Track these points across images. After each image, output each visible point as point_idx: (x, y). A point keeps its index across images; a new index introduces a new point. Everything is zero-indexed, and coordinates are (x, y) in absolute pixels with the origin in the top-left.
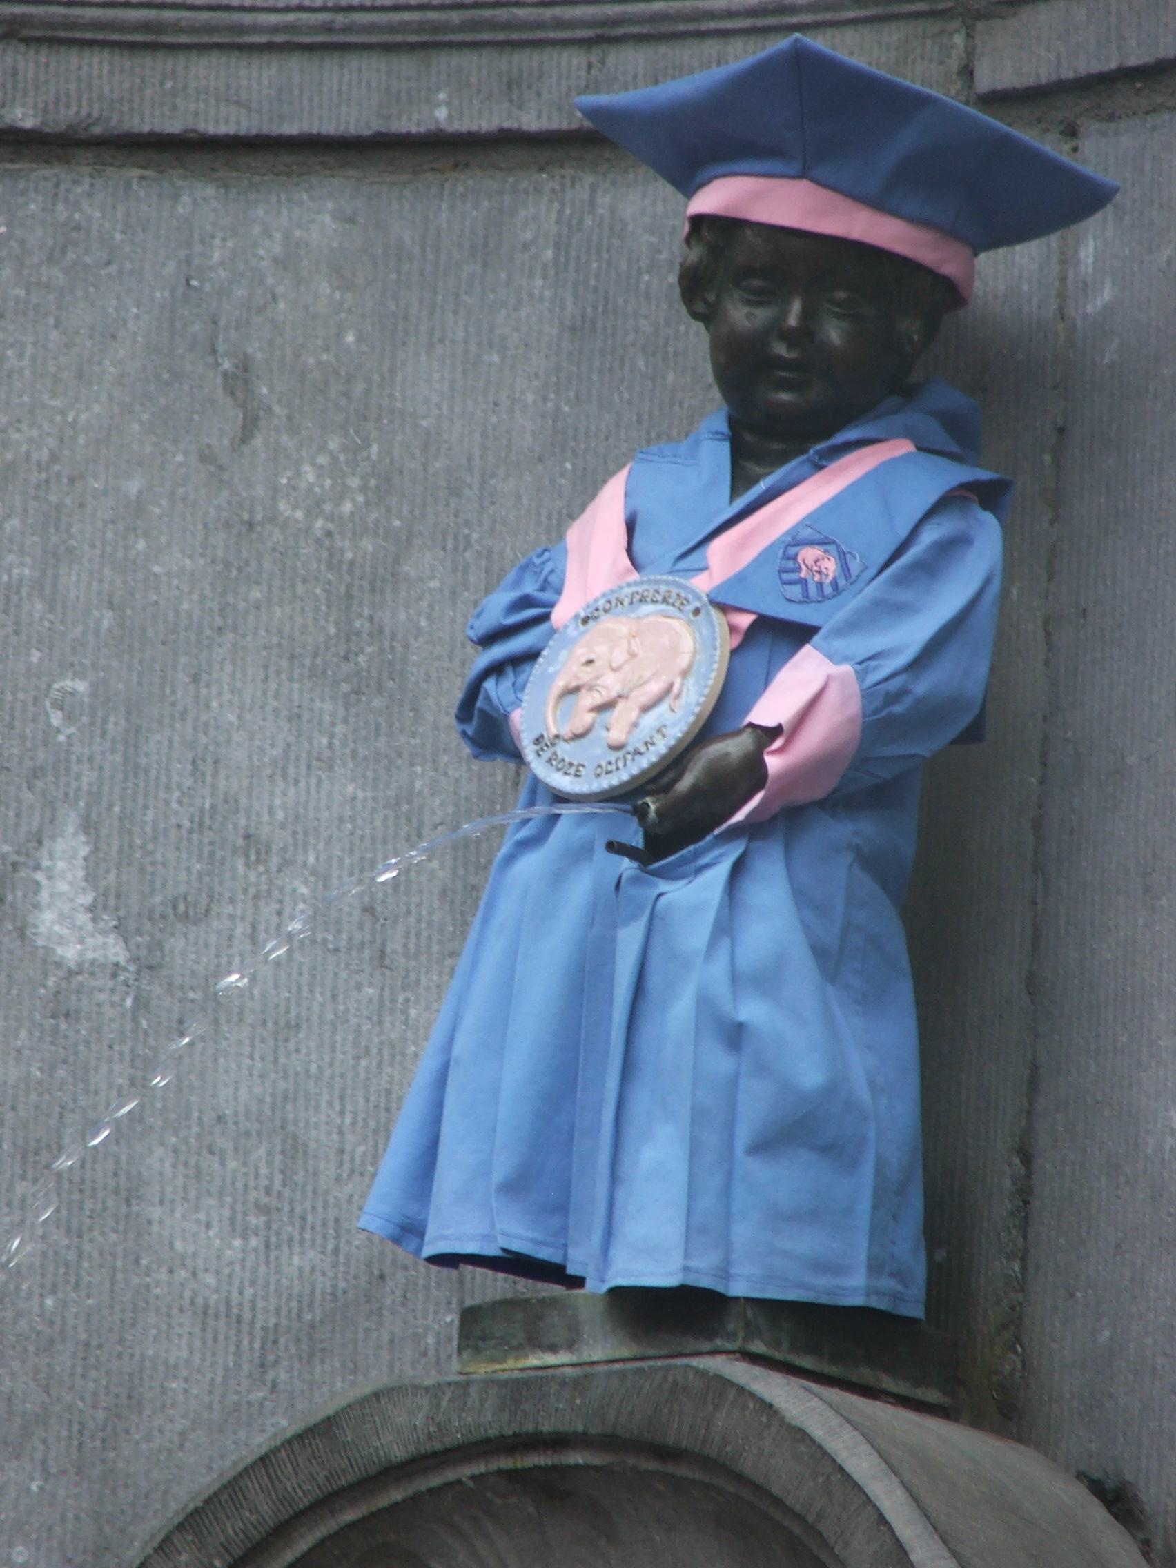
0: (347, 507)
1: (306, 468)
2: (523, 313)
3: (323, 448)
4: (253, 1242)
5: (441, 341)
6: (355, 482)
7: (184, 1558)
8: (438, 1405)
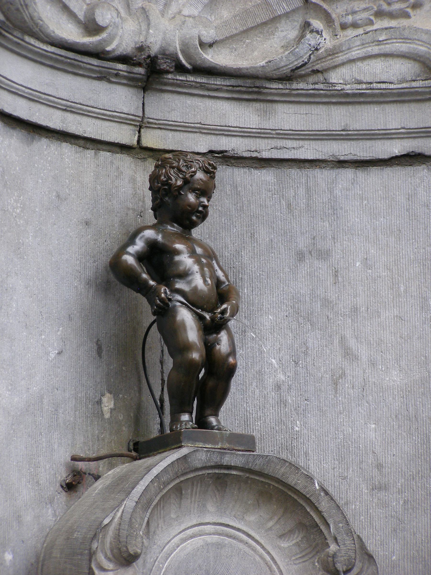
0: (18, 211)
1: (12, 199)
2: (45, 171)
3: (14, 195)
4: (10, 393)
5: (32, 174)
6: (19, 205)
7: (156, 484)
8: (207, 456)
